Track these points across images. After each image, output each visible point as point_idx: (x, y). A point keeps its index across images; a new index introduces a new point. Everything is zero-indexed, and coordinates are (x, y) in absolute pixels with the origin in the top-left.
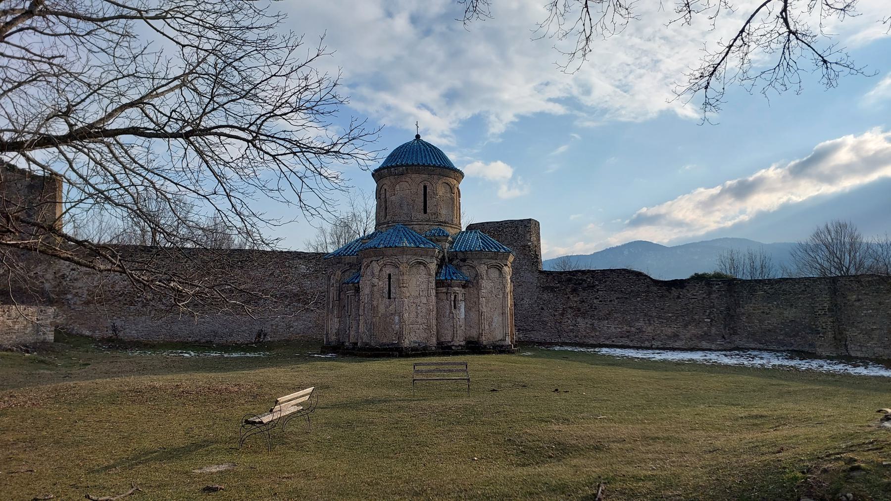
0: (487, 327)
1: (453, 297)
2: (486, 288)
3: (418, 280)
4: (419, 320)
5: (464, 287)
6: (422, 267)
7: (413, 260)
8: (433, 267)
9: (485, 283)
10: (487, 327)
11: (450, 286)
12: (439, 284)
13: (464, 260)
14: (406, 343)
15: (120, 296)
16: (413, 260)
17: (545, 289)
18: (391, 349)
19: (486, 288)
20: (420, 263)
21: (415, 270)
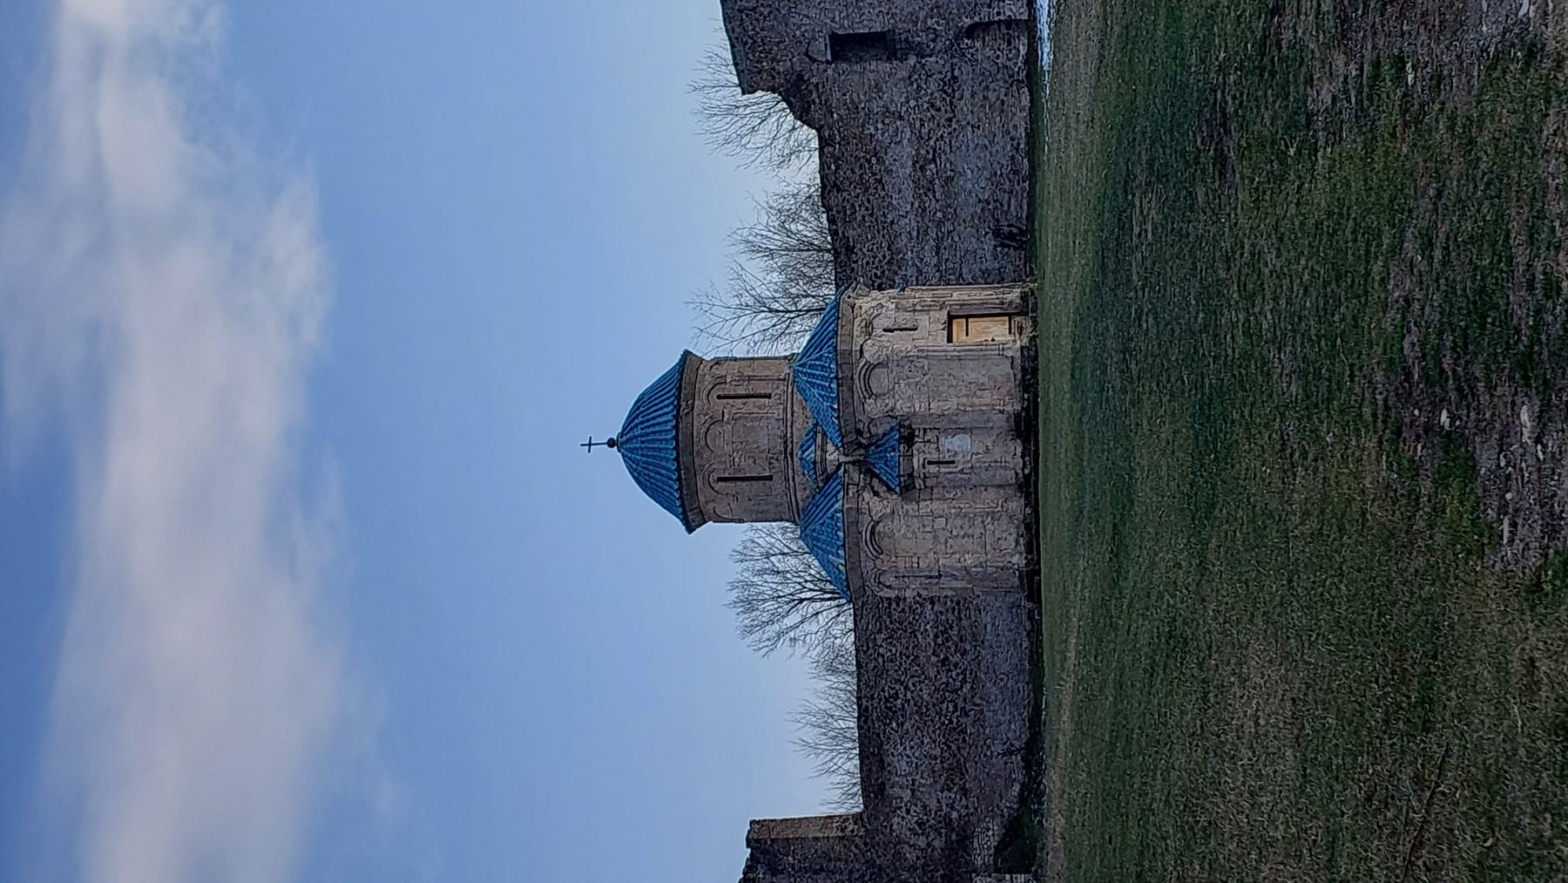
0: (987, 397)
1: (933, 469)
2: (911, 398)
3: (904, 536)
4: (978, 531)
5: (909, 440)
6: (880, 528)
7: (867, 549)
8: (876, 505)
9: (902, 407)
10: (987, 397)
11: (911, 476)
12: (907, 488)
13: (859, 432)
14: (1018, 560)
15: (949, 747)
16: (867, 549)
18: (1030, 582)
19: (911, 398)
20: (872, 533)
21: (885, 543)
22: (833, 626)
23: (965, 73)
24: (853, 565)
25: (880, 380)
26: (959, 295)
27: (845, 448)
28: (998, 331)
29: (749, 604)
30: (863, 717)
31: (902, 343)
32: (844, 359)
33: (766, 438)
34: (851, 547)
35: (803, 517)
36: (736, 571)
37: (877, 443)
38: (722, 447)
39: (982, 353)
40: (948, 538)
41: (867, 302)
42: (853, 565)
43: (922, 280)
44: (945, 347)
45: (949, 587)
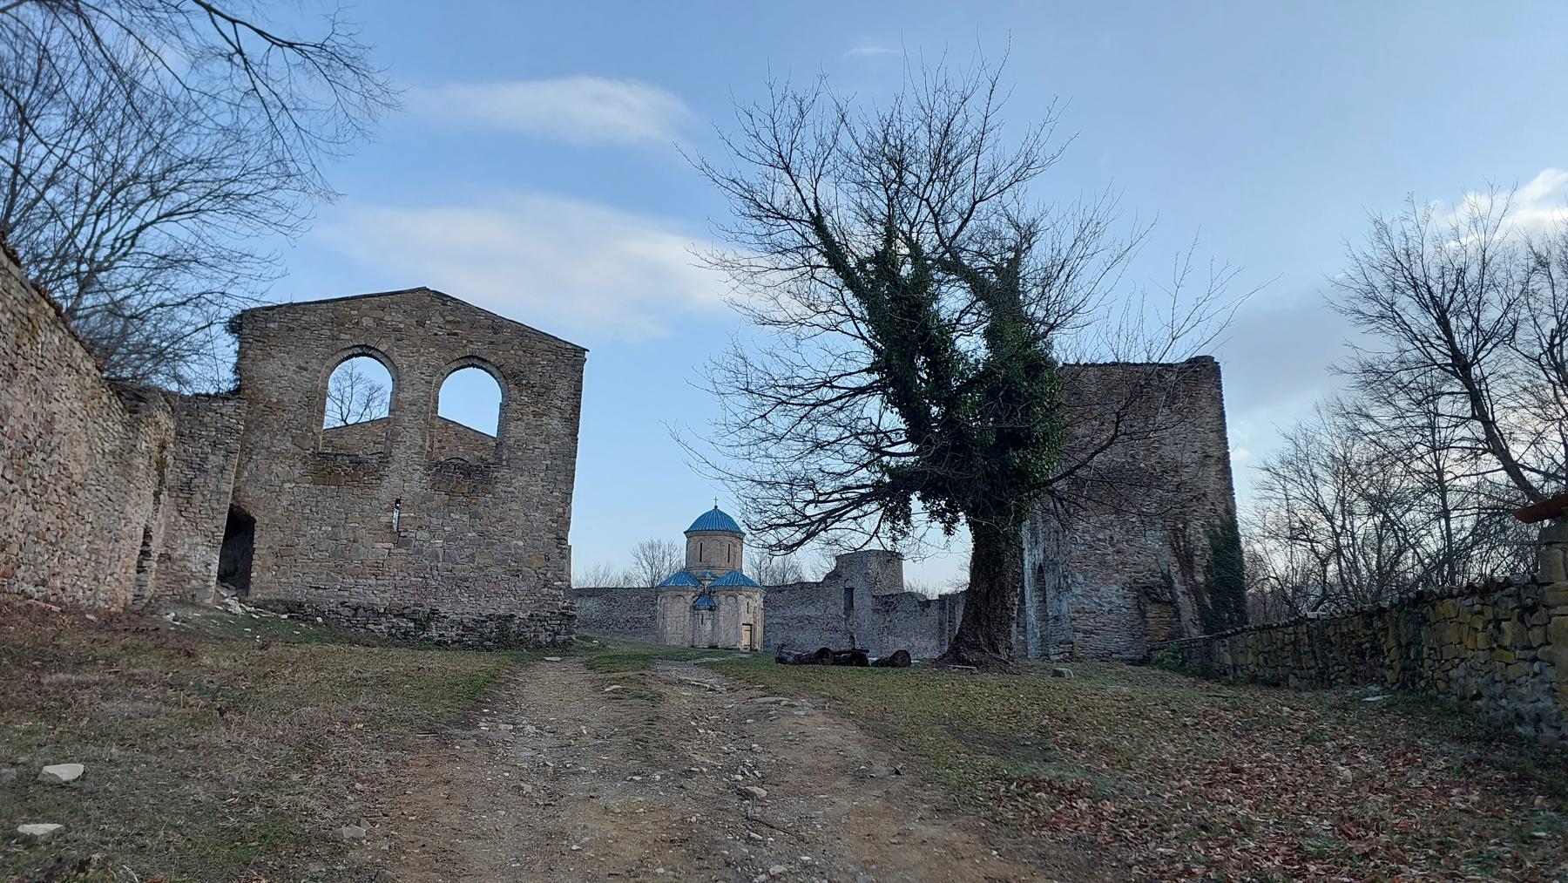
12: (694, 608)
17: (876, 611)
22: (641, 579)
23: (839, 635)
24: (670, 589)
25: (731, 600)
26: (759, 629)
27: (710, 587)
28: (745, 641)
29: (652, 547)
30: (609, 590)
31: (743, 608)
32: (739, 589)
33: (715, 561)
34: (675, 588)
35: (686, 573)
36: (665, 542)
37: (710, 598)
38: (711, 545)
39: (738, 635)
40: (676, 621)
41: (758, 600)
42: (670, 589)
43: (766, 617)
44: (742, 625)
45: (660, 621)
